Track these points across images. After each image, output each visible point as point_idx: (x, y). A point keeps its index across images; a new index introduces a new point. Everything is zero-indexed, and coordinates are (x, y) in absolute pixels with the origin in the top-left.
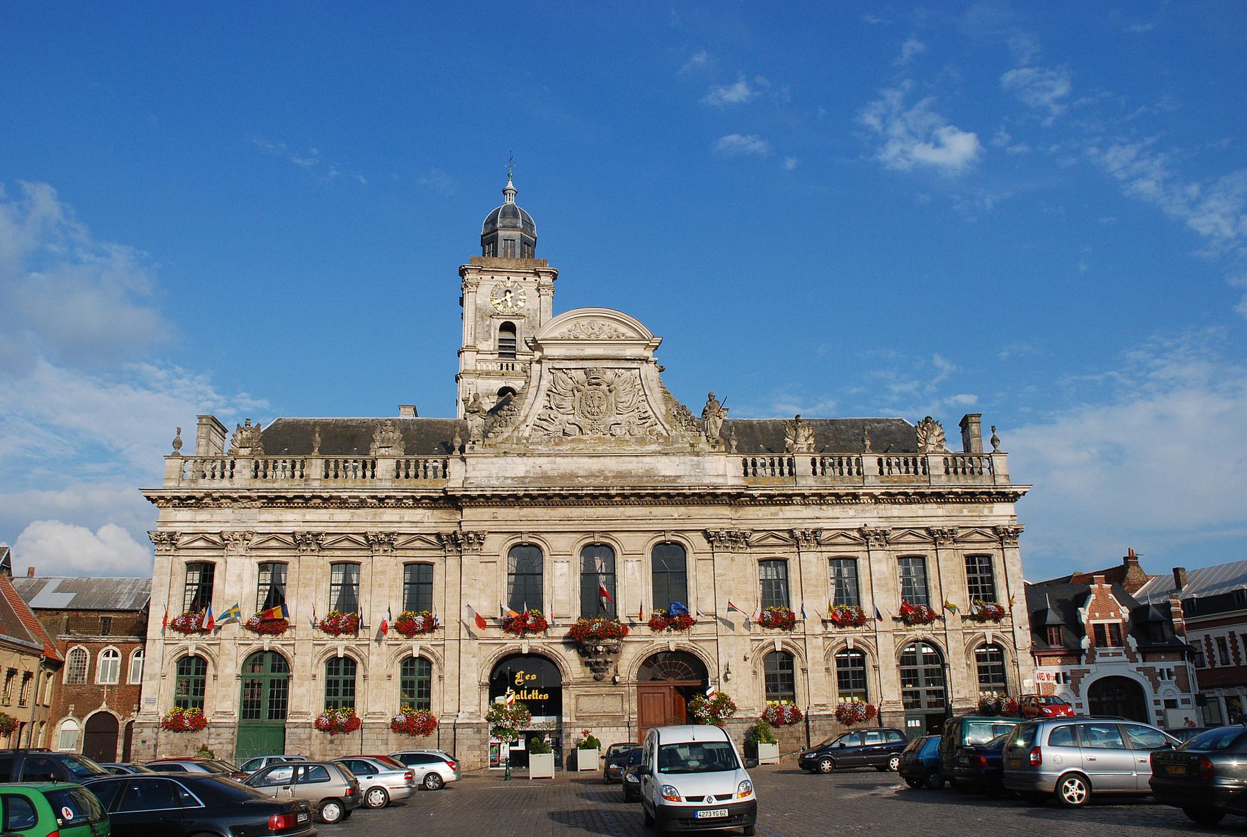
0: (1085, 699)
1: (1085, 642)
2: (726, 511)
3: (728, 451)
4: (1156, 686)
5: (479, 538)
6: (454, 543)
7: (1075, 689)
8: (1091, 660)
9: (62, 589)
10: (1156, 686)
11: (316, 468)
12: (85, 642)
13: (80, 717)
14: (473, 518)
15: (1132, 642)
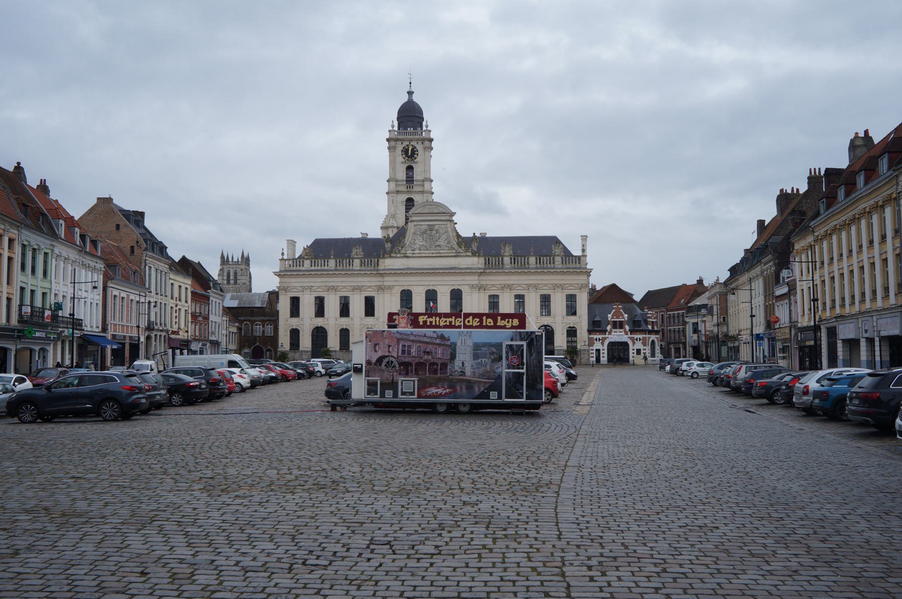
0: (606, 347)
1: (609, 328)
2: (476, 278)
3: (479, 256)
4: (634, 343)
5: (390, 288)
6: (380, 288)
7: (603, 344)
8: (610, 333)
9: (232, 298)
10: (634, 343)
11: (332, 263)
12: (248, 320)
13: (250, 347)
14: (388, 281)
15: (627, 328)
